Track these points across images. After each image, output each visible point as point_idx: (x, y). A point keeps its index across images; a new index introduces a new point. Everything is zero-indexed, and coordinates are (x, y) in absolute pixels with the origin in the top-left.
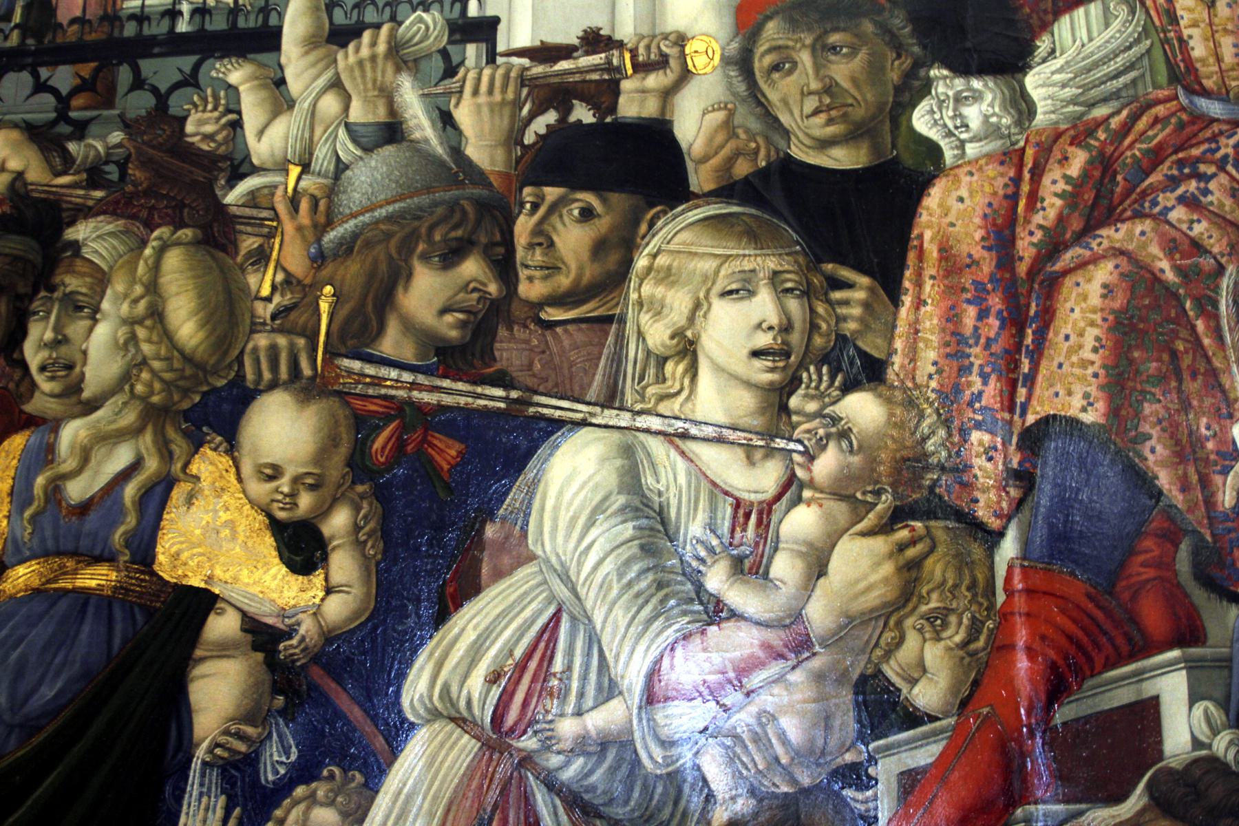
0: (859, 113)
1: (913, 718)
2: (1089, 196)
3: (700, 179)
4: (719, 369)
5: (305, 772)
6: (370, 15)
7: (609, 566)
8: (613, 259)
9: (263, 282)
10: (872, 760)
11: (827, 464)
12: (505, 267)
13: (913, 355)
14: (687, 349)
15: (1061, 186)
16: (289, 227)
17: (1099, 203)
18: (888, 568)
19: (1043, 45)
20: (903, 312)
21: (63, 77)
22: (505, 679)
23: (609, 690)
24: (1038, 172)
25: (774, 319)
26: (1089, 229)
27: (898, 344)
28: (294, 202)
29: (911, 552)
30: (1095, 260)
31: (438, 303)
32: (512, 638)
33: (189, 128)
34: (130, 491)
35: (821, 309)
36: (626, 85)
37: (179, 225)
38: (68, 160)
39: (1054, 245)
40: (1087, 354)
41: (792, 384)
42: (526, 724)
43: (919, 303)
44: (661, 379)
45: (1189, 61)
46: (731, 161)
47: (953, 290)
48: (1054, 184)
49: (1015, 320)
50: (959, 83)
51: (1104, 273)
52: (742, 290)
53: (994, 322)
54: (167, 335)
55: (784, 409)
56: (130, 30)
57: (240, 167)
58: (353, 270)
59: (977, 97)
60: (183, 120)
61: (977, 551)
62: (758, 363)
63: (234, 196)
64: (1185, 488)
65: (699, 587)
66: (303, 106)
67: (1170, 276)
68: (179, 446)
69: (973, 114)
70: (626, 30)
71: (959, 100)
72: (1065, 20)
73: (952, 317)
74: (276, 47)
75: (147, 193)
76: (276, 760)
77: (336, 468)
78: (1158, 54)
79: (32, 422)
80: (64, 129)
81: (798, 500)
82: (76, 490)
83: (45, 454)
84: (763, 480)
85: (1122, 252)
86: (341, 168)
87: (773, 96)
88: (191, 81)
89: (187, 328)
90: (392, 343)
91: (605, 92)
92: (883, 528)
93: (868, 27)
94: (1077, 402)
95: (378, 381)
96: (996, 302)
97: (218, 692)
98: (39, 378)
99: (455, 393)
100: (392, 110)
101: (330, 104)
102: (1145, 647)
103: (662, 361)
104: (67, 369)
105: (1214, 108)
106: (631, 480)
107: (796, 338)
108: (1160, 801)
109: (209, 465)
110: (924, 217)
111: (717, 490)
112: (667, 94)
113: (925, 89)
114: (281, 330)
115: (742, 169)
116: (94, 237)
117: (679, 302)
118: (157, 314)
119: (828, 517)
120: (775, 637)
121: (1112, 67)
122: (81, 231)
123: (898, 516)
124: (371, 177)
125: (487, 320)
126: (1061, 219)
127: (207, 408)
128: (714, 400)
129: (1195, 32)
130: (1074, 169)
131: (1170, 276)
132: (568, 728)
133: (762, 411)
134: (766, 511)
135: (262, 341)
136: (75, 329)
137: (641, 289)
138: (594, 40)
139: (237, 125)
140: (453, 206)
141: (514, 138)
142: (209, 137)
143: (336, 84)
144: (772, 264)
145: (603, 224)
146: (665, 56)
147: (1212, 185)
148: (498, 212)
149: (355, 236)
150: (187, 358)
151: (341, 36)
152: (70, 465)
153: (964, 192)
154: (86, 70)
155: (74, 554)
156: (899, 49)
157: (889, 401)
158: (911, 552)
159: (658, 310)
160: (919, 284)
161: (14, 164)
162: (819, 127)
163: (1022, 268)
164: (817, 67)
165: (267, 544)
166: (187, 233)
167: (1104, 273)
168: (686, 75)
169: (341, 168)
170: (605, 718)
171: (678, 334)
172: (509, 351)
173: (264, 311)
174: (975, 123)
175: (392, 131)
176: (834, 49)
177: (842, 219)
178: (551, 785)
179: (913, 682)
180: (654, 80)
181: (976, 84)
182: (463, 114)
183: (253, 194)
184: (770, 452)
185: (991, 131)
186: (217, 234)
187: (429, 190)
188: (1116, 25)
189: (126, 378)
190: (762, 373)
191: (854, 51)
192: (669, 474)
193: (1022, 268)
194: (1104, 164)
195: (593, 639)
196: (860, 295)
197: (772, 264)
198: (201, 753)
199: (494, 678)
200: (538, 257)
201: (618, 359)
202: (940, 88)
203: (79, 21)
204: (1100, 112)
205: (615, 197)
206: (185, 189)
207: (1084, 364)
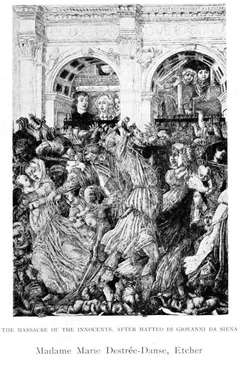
143: (206, 126)
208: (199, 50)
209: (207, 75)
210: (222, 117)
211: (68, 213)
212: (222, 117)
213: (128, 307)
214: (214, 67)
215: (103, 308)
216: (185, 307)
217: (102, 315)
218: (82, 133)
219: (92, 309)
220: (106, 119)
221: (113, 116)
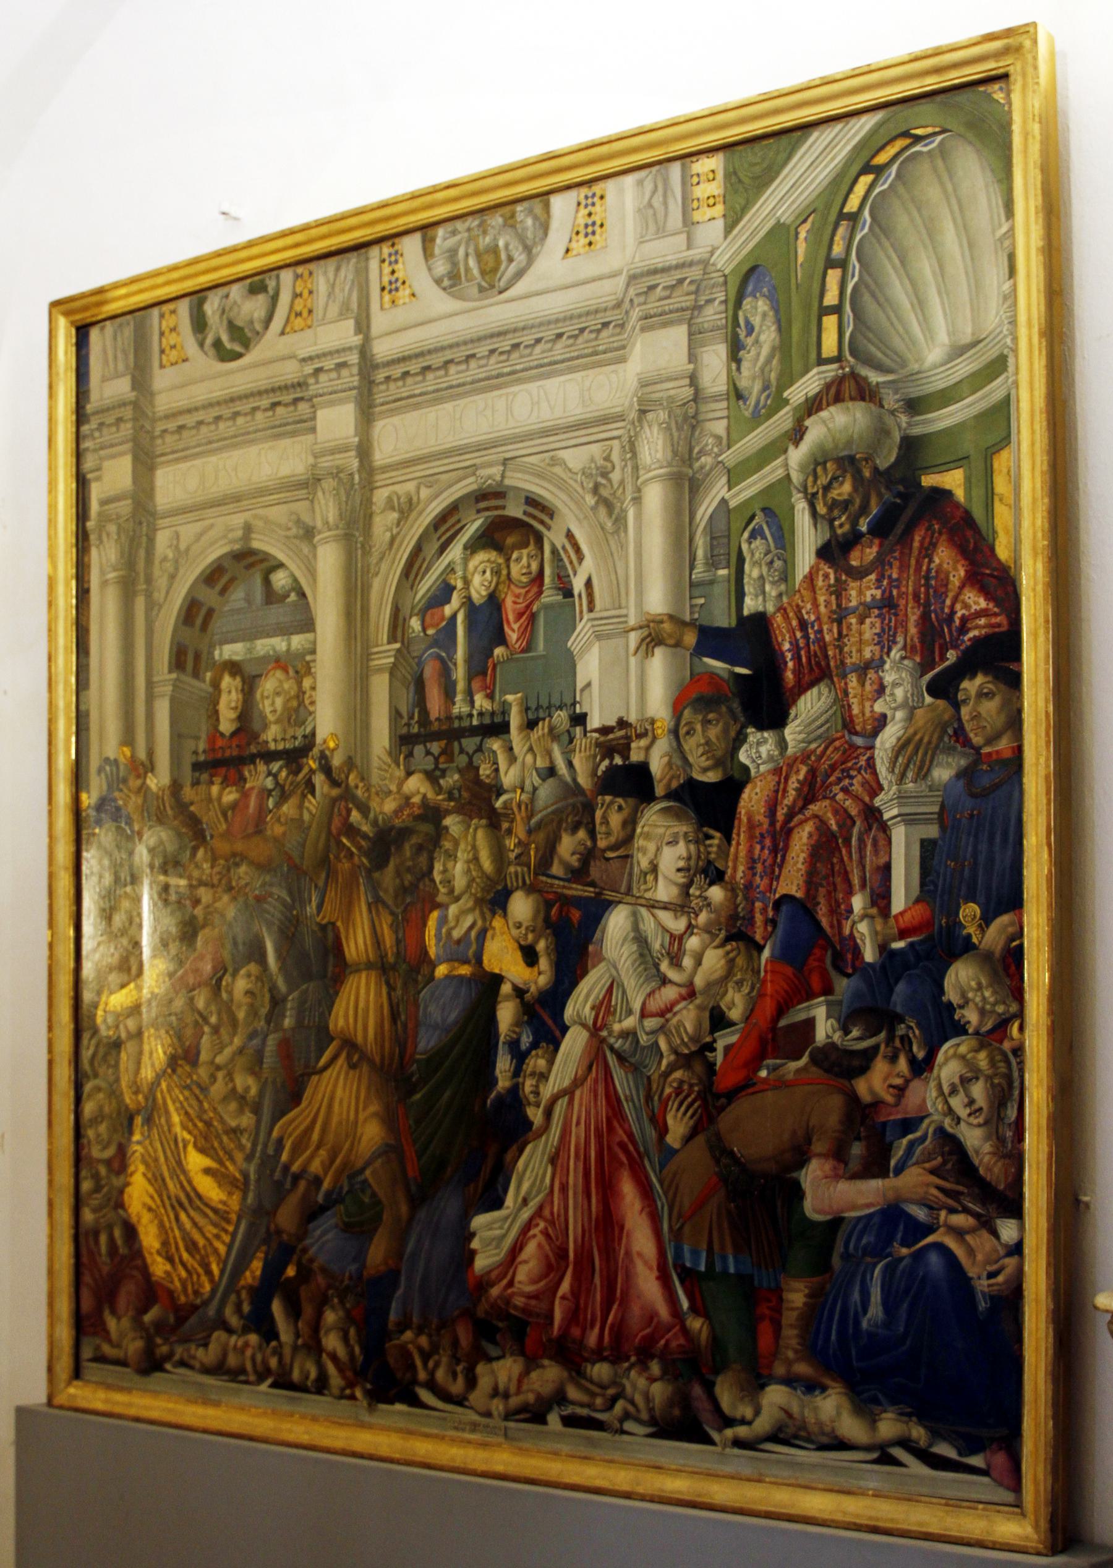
0: (719, 753)
1: (732, 1024)
2: (806, 789)
3: (659, 791)
4: (666, 877)
5: (535, 1045)
6: (541, 715)
7: (629, 962)
8: (629, 828)
9: (510, 843)
10: (715, 1041)
11: (703, 918)
12: (592, 834)
13: (735, 869)
14: (654, 869)
15: (796, 785)
16: (518, 818)
17: (810, 793)
18: (723, 962)
19: (793, 712)
20: (732, 849)
21: (435, 747)
22: (596, 1008)
23: (630, 1012)
24: (787, 779)
25: (685, 855)
26: (804, 807)
27: (730, 864)
28: (519, 806)
29: (731, 955)
30: (806, 820)
31: (571, 849)
32: (599, 992)
33: (481, 772)
34: (473, 934)
35: (702, 849)
36: (633, 745)
37: (481, 818)
38: (440, 788)
39: (790, 816)
40: (800, 866)
41: (690, 884)
42: (604, 1026)
43: (738, 844)
44: (645, 882)
45: (851, 716)
46: (670, 781)
47: (751, 837)
48: (793, 784)
49: (775, 851)
50: (759, 735)
51: (808, 828)
52: (673, 843)
53: (766, 852)
54: (480, 867)
55: (688, 894)
56: (456, 724)
57: (500, 791)
58: (541, 836)
59: (765, 741)
60: (478, 769)
61: (755, 954)
62: (680, 874)
63: (498, 804)
64: (832, 926)
65: (658, 970)
66: (520, 760)
67: (834, 827)
68: (488, 915)
69: (764, 750)
70: (632, 718)
71: (759, 744)
72: (803, 698)
73: (750, 851)
74: (508, 731)
75: (470, 803)
76: (526, 1040)
77: (540, 923)
78: (839, 714)
79: (438, 906)
80: (438, 773)
81: (692, 934)
82: (457, 934)
83: (443, 920)
84: (678, 925)
85: (816, 816)
86: (535, 789)
87: (686, 747)
88: (480, 749)
89: (487, 865)
90: (556, 869)
91: (624, 750)
92: (722, 945)
93: (724, 709)
94: (795, 888)
95: (552, 885)
96: (768, 842)
97: (506, 1014)
98: (440, 887)
99: (577, 890)
100: (551, 762)
101: (529, 758)
102: (810, 995)
103: (646, 874)
104: (448, 882)
105: (859, 741)
106: (636, 927)
107: (692, 863)
108: (813, 1060)
109: (498, 923)
110: (742, 803)
111: (665, 930)
112: (648, 749)
113: (744, 740)
114: (518, 864)
115: (674, 785)
116: (451, 822)
117: (651, 847)
118: (476, 859)
119: (702, 941)
120: (683, 991)
121: (818, 723)
122: (448, 821)
123: (728, 939)
124: (546, 792)
125: (589, 856)
126: (795, 801)
127: (495, 900)
128: (664, 892)
129: (855, 700)
130: (801, 777)
131: (834, 827)
132: (617, 1027)
133: (680, 895)
134: (681, 938)
135: (512, 869)
136: (450, 865)
137: (639, 842)
138: (622, 723)
139: (497, 770)
140: (574, 806)
141: (594, 773)
142: (488, 776)
144: (685, 829)
145: (625, 813)
146: (647, 731)
147: (855, 781)
148: (589, 808)
149: (541, 820)
150: (488, 878)
151: (531, 725)
152: (452, 924)
153: (758, 790)
154: (443, 743)
155: (457, 960)
156: (735, 720)
157: (726, 889)
158: (731, 955)
159: (644, 851)
160: (738, 835)
161: (422, 790)
162: (704, 762)
163: (778, 825)
164: (704, 731)
165: (519, 954)
166: (484, 822)
167: (808, 828)
168: (655, 739)
169: (535, 789)
170: (630, 1022)
171: (651, 862)
172: (595, 871)
173: (512, 856)
174: (764, 755)
175: (551, 771)
176: (709, 722)
177: (710, 805)
178: (612, 1048)
179: (730, 1009)
180: (643, 742)
181: (766, 735)
182: (576, 762)
183: (505, 803)
184: (683, 913)
185: (771, 758)
186: (494, 821)
187: (565, 798)
188: (823, 699)
189: (469, 886)
190: (681, 879)
191: (718, 721)
192: (648, 925)
193: (778, 825)
194: (812, 772)
195: (624, 992)
196: (716, 842)
197: (685, 829)
198: (502, 1039)
199: (593, 1008)
200: (603, 829)
201: (631, 874)
202: (751, 739)
203: (438, 719)
204: (813, 746)
205: (631, 801)
206: (481, 799)
207: (799, 870)
208: (517, 480)
209: (534, 566)
210: (578, 711)
211: (198, 1053)
212: (578, 711)
213: (331, 1369)
214: (554, 537)
215: (273, 1362)
216: (472, 1382)
218: (230, 796)
219: (249, 1366)
220: (281, 747)
221: (299, 733)
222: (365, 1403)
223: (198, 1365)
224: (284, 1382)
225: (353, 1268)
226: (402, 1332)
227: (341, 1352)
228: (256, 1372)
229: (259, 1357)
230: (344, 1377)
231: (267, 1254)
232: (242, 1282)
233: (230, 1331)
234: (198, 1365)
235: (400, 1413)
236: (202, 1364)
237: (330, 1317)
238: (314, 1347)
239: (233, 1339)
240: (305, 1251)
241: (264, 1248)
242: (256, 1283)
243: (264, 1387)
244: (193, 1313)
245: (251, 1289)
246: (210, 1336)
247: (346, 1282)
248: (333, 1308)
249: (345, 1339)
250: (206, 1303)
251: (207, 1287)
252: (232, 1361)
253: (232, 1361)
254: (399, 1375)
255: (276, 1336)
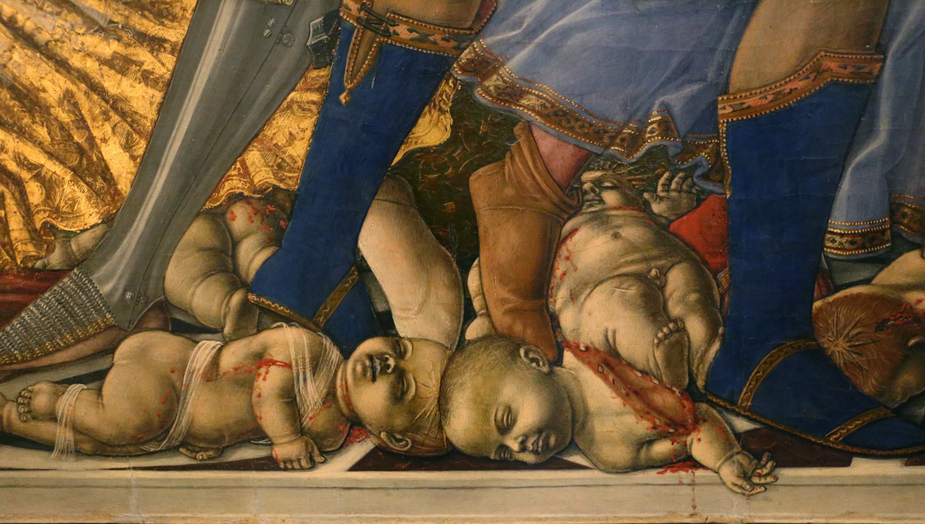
213: (596, 391)
215: (372, 399)
217: (359, 466)
219: (272, 418)
222: (728, 473)
223: (63, 435)
224: (415, 448)
225: (677, 98)
226: (884, 261)
227: (636, 341)
228: (299, 430)
229: (312, 392)
230: (648, 410)
231: (331, 91)
232: (234, 184)
233: (189, 328)
234: (63, 435)
235: (870, 484)
236: (77, 429)
237: (589, 247)
238: (536, 334)
239: (206, 348)
240: (483, 67)
241: (319, 75)
242: (292, 181)
243: (336, 469)
244: (34, 293)
245: (267, 200)
246: (110, 350)
247: (653, 139)
248: (601, 219)
249: (653, 303)
250: (82, 262)
251: (90, 214)
252: (202, 409)
253: (202, 409)
254: (869, 385)
255: (383, 324)
